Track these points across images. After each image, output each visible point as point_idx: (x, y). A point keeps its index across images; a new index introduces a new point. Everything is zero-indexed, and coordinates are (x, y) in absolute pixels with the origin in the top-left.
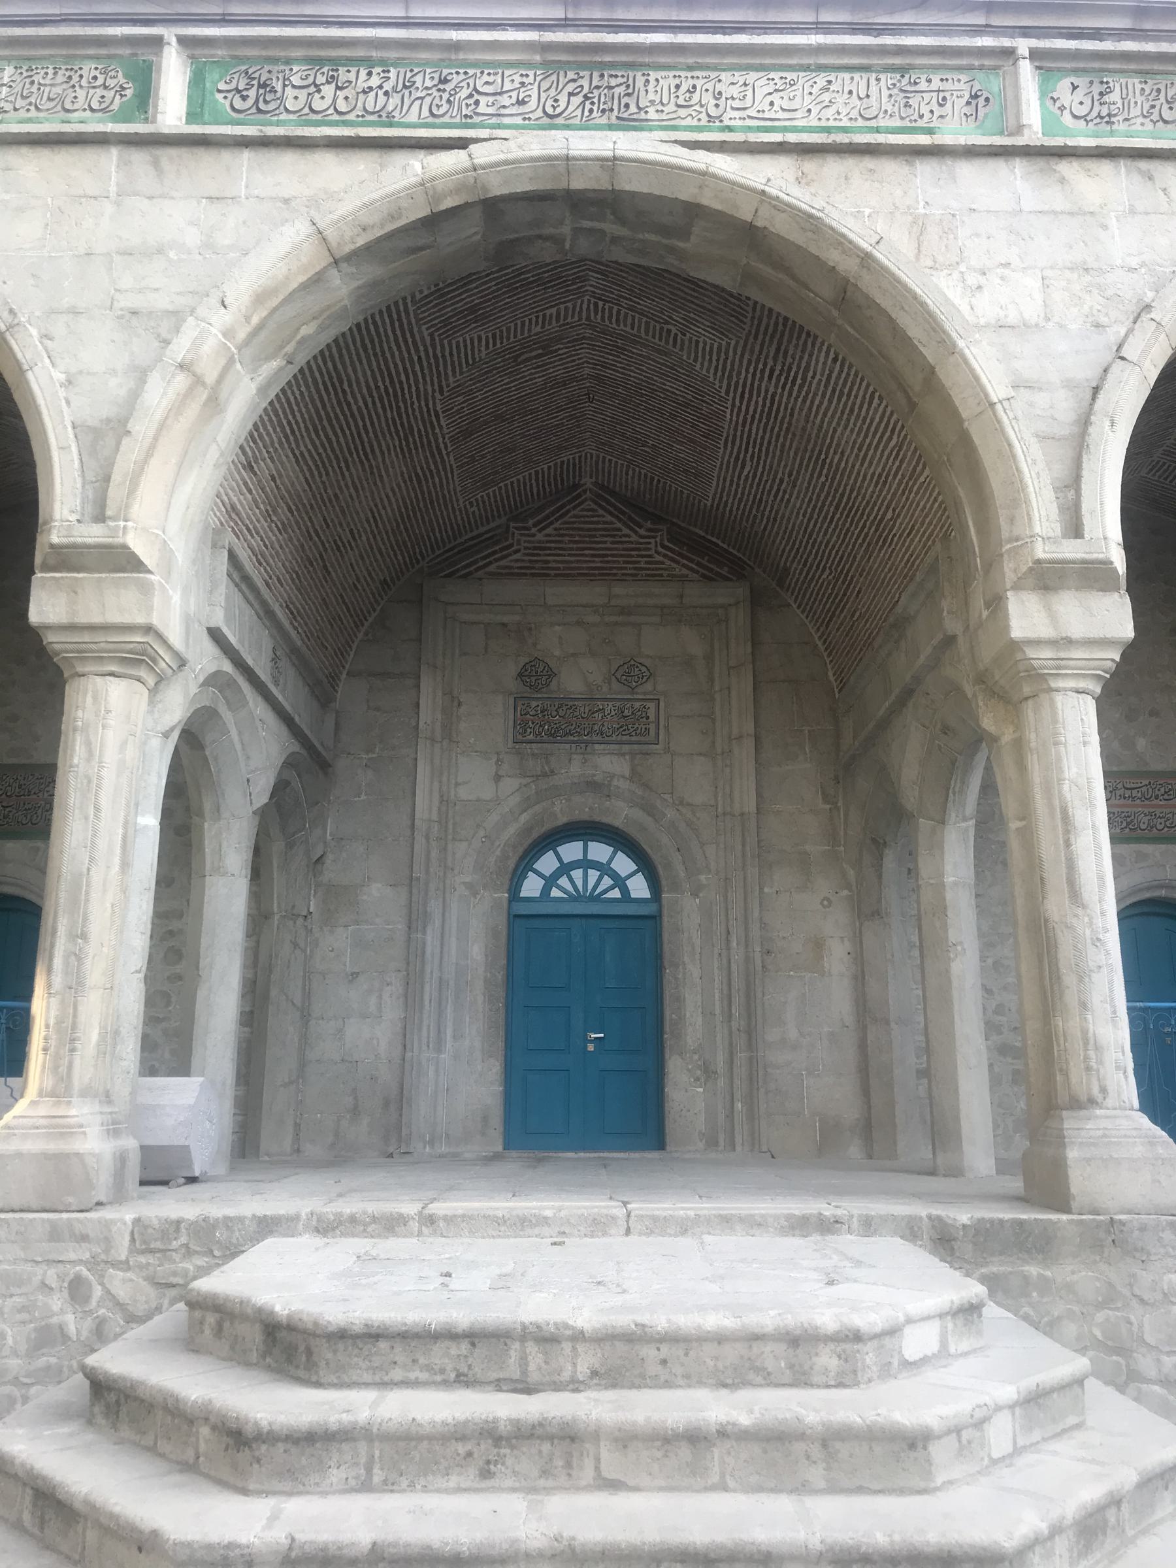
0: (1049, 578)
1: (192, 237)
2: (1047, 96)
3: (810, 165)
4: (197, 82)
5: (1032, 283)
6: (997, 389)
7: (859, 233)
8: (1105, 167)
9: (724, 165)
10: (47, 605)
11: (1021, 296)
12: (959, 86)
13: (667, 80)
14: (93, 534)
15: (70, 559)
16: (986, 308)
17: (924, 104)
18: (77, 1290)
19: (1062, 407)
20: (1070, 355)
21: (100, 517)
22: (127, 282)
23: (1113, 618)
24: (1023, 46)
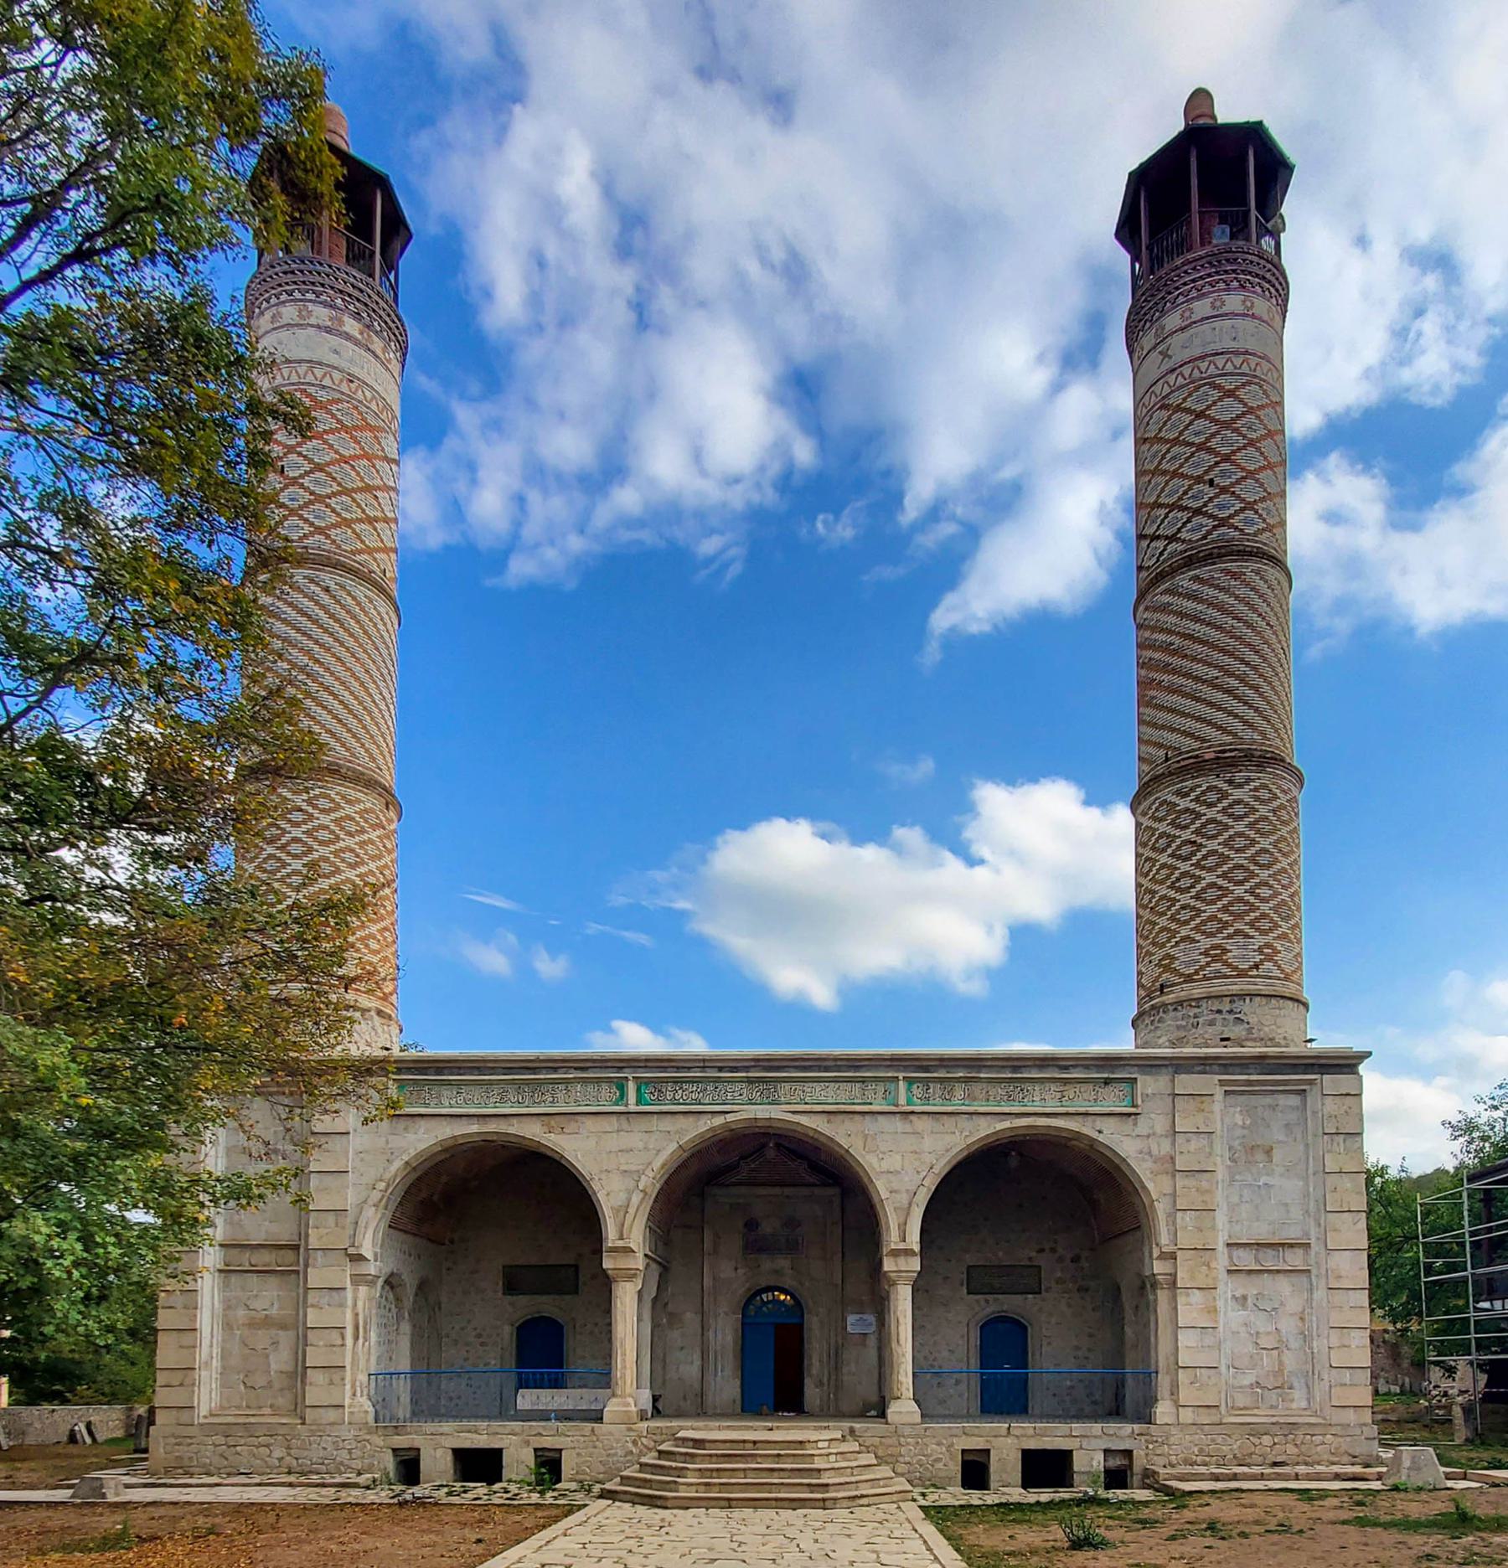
0: (896, 1253)
1: (641, 1145)
2: (909, 1090)
3: (832, 1117)
4: (638, 1090)
5: (899, 1157)
6: (884, 1194)
7: (844, 1142)
8: (925, 1117)
9: (804, 1120)
10: (607, 1264)
11: (894, 1162)
12: (881, 1088)
13: (787, 1086)
14: (620, 1243)
15: (615, 1250)
16: (885, 1166)
17: (869, 1094)
18: (635, 1443)
19: (904, 1199)
20: (909, 1181)
21: (621, 1238)
22: (622, 1161)
23: (915, 1264)
24: (901, 1075)
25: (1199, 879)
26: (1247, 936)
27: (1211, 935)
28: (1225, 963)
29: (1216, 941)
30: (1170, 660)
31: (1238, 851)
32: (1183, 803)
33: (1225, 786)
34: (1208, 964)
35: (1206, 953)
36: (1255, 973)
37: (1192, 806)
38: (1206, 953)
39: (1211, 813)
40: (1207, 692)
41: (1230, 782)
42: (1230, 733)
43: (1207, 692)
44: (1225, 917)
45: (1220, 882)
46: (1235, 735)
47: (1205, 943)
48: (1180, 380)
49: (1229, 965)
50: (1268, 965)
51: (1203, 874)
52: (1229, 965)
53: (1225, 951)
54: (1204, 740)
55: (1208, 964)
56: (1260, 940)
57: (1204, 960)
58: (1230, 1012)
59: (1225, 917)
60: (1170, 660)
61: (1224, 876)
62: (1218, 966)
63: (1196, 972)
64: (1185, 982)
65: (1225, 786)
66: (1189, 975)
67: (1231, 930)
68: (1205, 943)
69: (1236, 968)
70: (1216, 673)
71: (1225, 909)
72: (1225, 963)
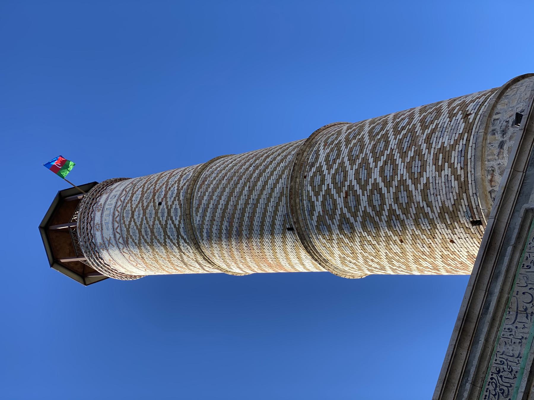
25: (375, 185)
26: (433, 131)
27: (423, 167)
28: (453, 147)
29: (430, 160)
30: (235, 229)
31: (361, 151)
32: (319, 208)
33: (314, 169)
34: (451, 166)
35: (440, 169)
36: (471, 117)
37: (320, 198)
38: (440, 169)
39: (328, 180)
40: (255, 194)
41: (313, 165)
42: (283, 172)
43: (255, 194)
44: (411, 154)
45: (380, 164)
46: (286, 167)
47: (431, 171)
48: (118, 230)
49: (456, 142)
50: (470, 108)
51: (371, 181)
52: (456, 142)
53: (442, 149)
54: (282, 194)
55: (451, 166)
56: (444, 119)
57: (447, 171)
58: (504, 132)
59: (411, 154)
60: (235, 229)
61: (376, 160)
62: (454, 154)
63: (457, 178)
64: (466, 191)
65: (314, 169)
66: (460, 187)
67: (424, 146)
68: (431, 171)
69: (461, 136)
70: (246, 188)
71: (403, 155)
72: (453, 147)
